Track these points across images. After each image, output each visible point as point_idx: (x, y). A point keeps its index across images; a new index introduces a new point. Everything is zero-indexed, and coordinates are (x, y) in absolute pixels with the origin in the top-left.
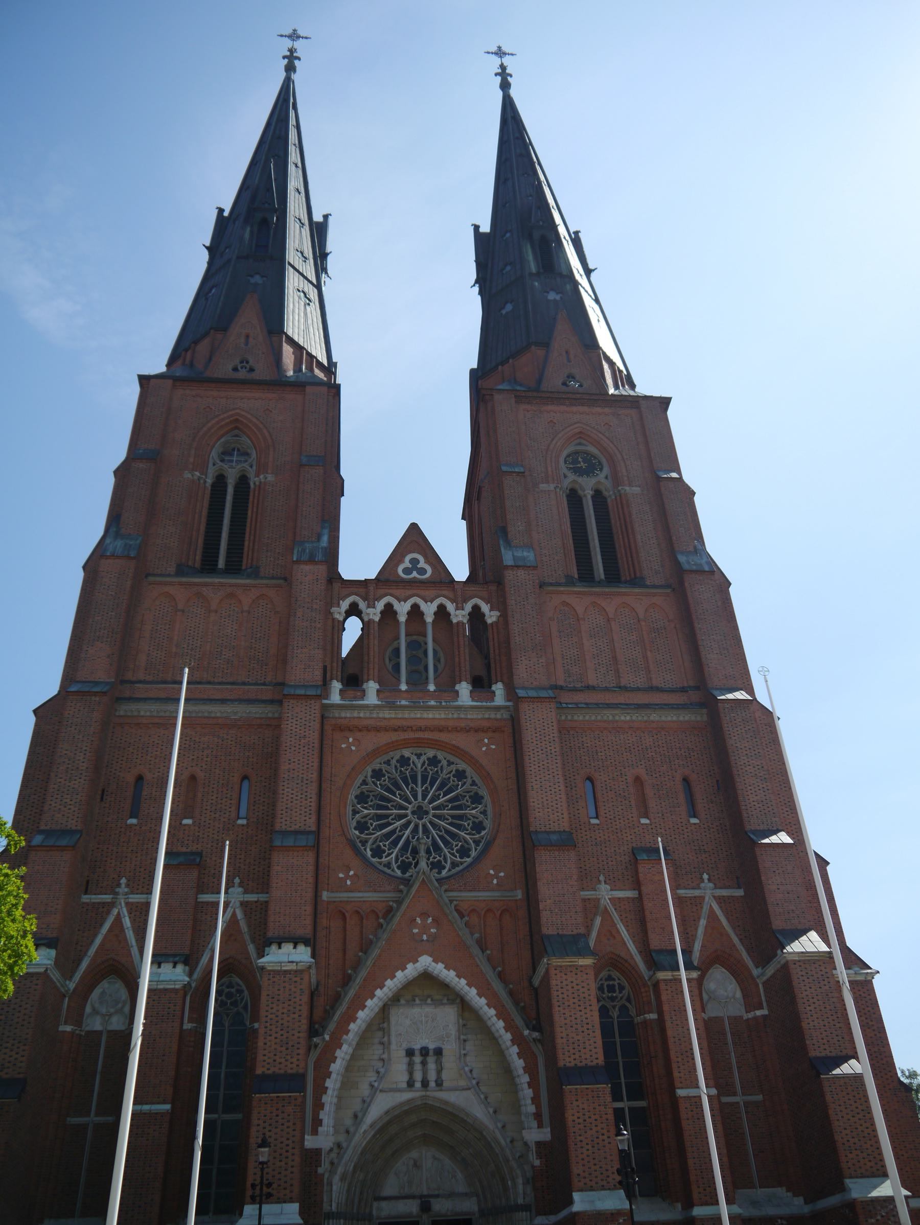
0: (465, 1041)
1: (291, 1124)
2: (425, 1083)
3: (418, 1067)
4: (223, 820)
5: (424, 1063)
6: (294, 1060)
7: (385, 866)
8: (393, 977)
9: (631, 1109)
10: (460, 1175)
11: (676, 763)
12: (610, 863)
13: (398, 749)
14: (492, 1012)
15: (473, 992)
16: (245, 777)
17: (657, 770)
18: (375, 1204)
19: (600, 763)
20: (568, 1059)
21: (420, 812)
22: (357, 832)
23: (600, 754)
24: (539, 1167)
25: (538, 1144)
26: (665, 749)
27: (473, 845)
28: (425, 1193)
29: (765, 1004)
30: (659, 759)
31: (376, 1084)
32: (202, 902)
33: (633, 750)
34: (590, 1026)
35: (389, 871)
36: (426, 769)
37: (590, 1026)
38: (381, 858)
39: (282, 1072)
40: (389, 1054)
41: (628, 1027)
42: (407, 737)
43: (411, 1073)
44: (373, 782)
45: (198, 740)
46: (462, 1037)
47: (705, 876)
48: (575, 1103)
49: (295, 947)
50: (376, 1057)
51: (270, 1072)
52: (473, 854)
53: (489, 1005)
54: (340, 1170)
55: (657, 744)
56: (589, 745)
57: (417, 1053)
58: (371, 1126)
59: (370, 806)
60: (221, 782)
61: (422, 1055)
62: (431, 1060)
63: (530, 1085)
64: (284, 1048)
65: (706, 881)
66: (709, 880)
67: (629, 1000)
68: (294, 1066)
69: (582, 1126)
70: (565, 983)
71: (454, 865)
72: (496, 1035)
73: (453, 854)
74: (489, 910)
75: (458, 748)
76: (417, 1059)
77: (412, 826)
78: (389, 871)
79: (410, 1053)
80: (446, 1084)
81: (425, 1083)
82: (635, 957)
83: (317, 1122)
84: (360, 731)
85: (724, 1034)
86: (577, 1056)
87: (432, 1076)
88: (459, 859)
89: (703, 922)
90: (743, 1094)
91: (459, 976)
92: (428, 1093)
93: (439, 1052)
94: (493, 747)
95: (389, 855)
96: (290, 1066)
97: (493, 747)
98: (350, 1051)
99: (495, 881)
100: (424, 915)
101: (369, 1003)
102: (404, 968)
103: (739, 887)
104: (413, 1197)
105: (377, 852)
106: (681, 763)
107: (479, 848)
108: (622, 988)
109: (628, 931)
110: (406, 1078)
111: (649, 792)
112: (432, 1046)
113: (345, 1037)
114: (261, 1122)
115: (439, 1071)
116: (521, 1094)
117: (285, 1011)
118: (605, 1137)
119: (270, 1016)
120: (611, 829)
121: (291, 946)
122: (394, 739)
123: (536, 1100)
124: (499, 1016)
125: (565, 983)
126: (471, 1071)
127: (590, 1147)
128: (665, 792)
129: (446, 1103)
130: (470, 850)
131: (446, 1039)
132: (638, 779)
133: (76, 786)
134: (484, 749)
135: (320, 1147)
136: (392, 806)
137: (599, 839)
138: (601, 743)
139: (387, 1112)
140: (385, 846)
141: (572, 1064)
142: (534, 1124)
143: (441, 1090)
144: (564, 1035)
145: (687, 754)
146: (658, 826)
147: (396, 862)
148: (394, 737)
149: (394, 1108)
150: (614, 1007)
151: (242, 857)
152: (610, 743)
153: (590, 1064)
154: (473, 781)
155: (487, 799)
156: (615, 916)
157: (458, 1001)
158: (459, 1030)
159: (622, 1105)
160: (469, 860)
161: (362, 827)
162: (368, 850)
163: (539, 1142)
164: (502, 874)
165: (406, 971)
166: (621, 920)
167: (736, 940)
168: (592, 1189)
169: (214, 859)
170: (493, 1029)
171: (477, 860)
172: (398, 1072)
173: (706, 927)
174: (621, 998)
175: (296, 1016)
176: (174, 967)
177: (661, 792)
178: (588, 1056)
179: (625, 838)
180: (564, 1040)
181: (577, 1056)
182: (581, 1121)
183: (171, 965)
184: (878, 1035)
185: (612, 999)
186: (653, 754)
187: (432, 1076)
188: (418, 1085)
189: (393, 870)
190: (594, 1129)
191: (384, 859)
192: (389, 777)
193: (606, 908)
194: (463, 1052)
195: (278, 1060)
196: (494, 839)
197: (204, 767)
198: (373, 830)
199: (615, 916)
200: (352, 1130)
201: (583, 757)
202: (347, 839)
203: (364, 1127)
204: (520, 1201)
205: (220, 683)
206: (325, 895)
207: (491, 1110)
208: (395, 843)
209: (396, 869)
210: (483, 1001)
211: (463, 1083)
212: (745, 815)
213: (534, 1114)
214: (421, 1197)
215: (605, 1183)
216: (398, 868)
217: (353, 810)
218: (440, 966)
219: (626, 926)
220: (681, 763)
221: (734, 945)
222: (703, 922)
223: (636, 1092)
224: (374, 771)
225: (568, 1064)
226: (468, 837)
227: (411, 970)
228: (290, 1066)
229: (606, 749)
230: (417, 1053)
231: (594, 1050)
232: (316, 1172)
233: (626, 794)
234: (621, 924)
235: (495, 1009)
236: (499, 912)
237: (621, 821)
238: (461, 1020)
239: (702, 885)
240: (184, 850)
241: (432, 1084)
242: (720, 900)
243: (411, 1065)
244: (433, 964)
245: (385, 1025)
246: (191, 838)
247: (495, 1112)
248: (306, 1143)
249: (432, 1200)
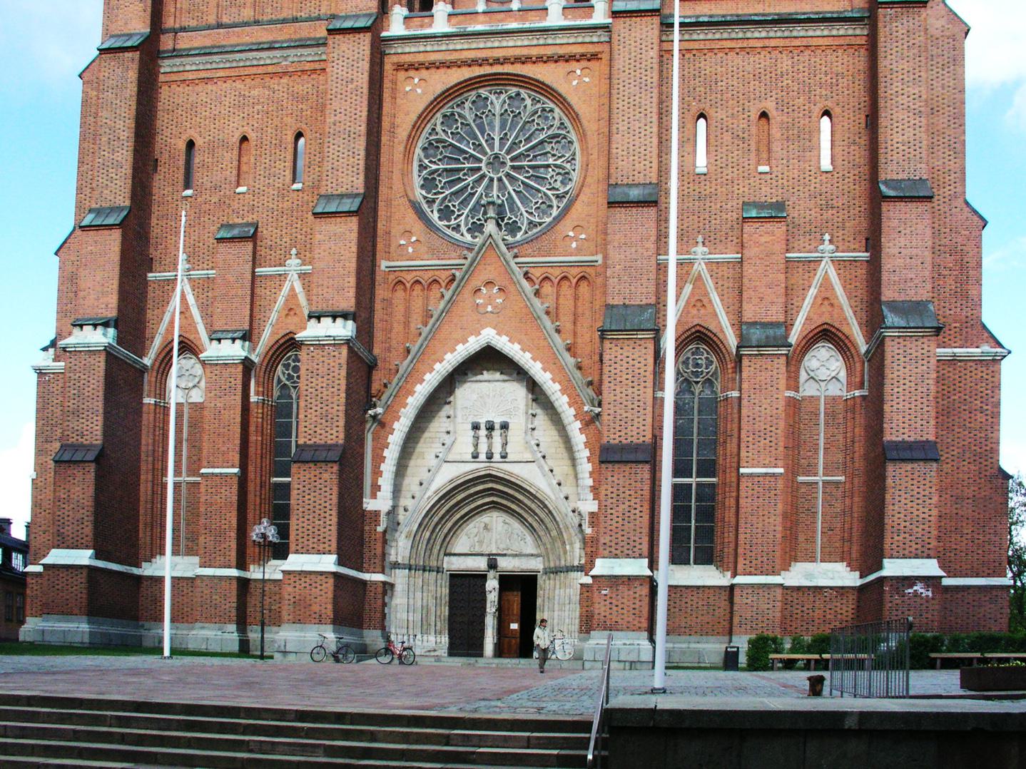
0: (534, 416)
1: (328, 489)
2: (490, 456)
3: (483, 440)
4: (277, 185)
5: (489, 437)
6: (334, 432)
7: (453, 229)
8: (453, 350)
9: (698, 485)
11: (817, 92)
12: (713, 222)
13: (473, 89)
14: (557, 387)
15: (538, 365)
16: (299, 135)
17: (791, 103)
19: (719, 96)
20: (612, 436)
21: (496, 161)
22: (424, 192)
23: (719, 84)
26: (806, 74)
27: (555, 203)
29: (866, 384)
30: (796, 89)
31: (440, 455)
32: (261, 276)
33: (763, 77)
34: (641, 404)
35: (457, 236)
36: (506, 110)
37: (641, 404)
38: (449, 220)
39: (322, 442)
40: (455, 424)
41: (710, 406)
42: (482, 73)
43: (476, 446)
44: (444, 131)
45: (247, 94)
46: (530, 412)
47: (827, 237)
48: (610, 478)
49: (334, 321)
50: (444, 430)
51: (311, 442)
52: (555, 212)
53: (553, 380)
55: (796, 69)
56: (707, 72)
57: (483, 426)
59: (440, 160)
60: (274, 142)
61: (487, 429)
62: (497, 433)
64: (323, 421)
65: (827, 242)
66: (831, 241)
67: (715, 373)
68: (333, 437)
69: (614, 500)
70: (620, 357)
71: (532, 224)
72: (560, 410)
73: (531, 214)
74: (565, 278)
75: (543, 83)
76: (483, 432)
77: (486, 181)
78: (457, 236)
79: (476, 427)
80: (510, 458)
81: (490, 456)
82: (725, 330)
83: (376, 488)
84: (427, 68)
85: (817, 415)
86: (622, 434)
87: (497, 450)
88: (537, 220)
89: (812, 292)
90: (824, 475)
91: (523, 350)
93: (505, 426)
94: (587, 80)
95: (459, 216)
96: (330, 437)
97: (587, 80)
99: (574, 245)
100: (489, 283)
101: (428, 377)
102: (465, 341)
103: (867, 251)
105: (446, 213)
106: (824, 93)
107: (562, 206)
108: (710, 363)
109: (722, 300)
110: (472, 449)
111: (776, 132)
112: (498, 421)
114: (300, 486)
115: (505, 444)
117: (324, 385)
118: (637, 511)
119: (310, 390)
120: (719, 180)
121: (329, 320)
122: (467, 76)
124: (563, 391)
125: (620, 357)
126: (538, 445)
127: (620, 519)
128: (796, 132)
129: (511, 474)
130: (551, 207)
132: (764, 115)
133: (119, 159)
134: (575, 83)
136: (465, 158)
137: (703, 193)
138: (724, 69)
140: (454, 206)
141: (616, 441)
142: (591, 496)
144: (612, 412)
145: (834, 80)
146: (780, 176)
147: (466, 225)
148: (466, 73)
150: (697, 383)
151: (298, 226)
152: (735, 69)
153: (635, 441)
154: (562, 124)
155: (576, 145)
156: (710, 284)
158: (527, 405)
159: (693, 480)
160: (548, 220)
161: (428, 184)
162: (435, 212)
164: (583, 236)
165: (467, 345)
166: (717, 288)
167: (849, 313)
168: (616, 556)
169: (270, 229)
170: (556, 404)
171: (558, 220)
172: (464, 446)
173: (816, 297)
174: (708, 373)
175: (335, 390)
176: (233, 342)
177: (791, 132)
178: (634, 433)
179: (737, 192)
180: (611, 418)
181: (622, 434)
182: (614, 495)
183: (230, 341)
184: (990, 420)
185: (696, 374)
186: (790, 82)
187: (497, 450)
188: (483, 457)
189: (462, 235)
190: (627, 503)
191: (453, 222)
192: (462, 123)
193: (700, 275)
194: (530, 426)
195: (319, 432)
196: (578, 196)
197: (256, 125)
198: (442, 188)
199: (710, 284)
200: (417, 495)
201: (697, 89)
202: (410, 201)
203: (429, 493)
205: (271, 22)
206: (384, 265)
207: (555, 482)
208: (464, 203)
209: (465, 233)
210: (548, 375)
211: (528, 457)
212: (884, 161)
215: (630, 552)
216: (469, 230)
217: (420, 166)
218: (505, 339)
219: (721, 296)
220: (824, 93)
221: (846, 319)
222: (812, 292)
223: (708, 468)
224: (445, 116)
225: (612, 441)
226: (549, 193)
227: (473, 345)
228: (330, 437)
229: (729, 76)
230: (483, 426)
231: (642, 428)
233: (745, 135)
234: (715, 293)
235: (560, 383)
236: (575, 280)
237: (735, 169)
238: (530, 396)
239: (821, 247)
240: (240, 221)
241: (497, 457)
242: (838, 263)
243: (477, 438)
244: (497, 337)
246: (246, 208)
248: (365, 506)
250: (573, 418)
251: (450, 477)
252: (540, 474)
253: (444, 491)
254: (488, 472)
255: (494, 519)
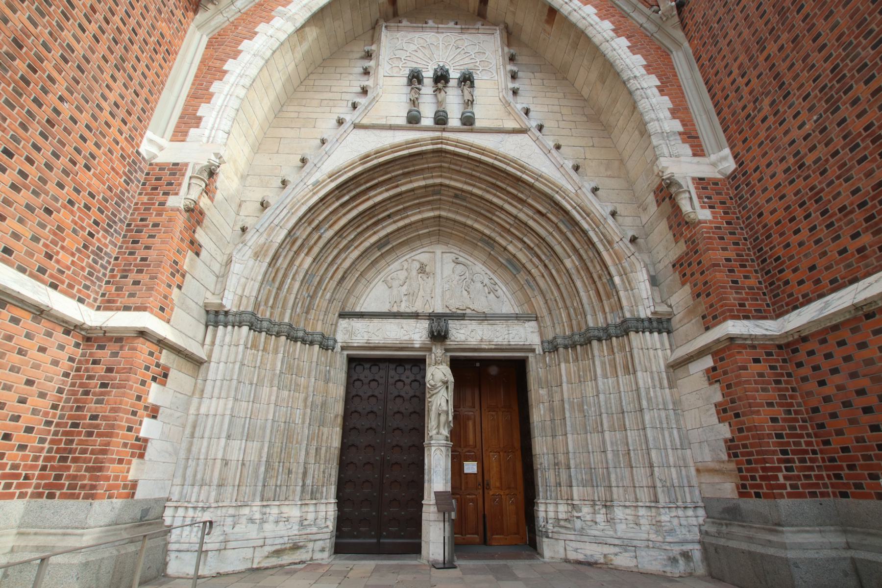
2: (441, 120)
10: (503, 289)
18: (344, 323)
24: (711, 222)
25: (701, 182)
28: (439, 309)
54: (253, 239)
57: (428, 81)
58: (332, 176)
63: (661, 90)
72: (581, 24)
76: (428, 88)
79: (415, 78)
80: (478, 124)
81: (441, 120)
92: (446, 135)
93: (467, 80)
98: (290, 28)
104: (416, 316)
113: (280, 8)
116: (643, 105)
123: (679, 110)
129: (482, 151)
131: (481, 69)
135: (186, 161)
139: (366, 158)
143: (472, 131)
149: (378, 153)
157: (502, 26)
163: (701, 179)
188: (427, 120)
200: (292, 178)
203: (318, 176)
204: (645, 312)
207: (569, 164)
213: (680, 134)
214: (433, 317)
232: (162, 204)
238: (506, 49)
241: (454, 121)
245: (374, 47)
247: (576, 168)
249: (452, 325)
250: (612, 34)
251: (364, 151)
252: (538, 150)
253: (351, 174)
254: (439, 146)
255: (438, 252)
